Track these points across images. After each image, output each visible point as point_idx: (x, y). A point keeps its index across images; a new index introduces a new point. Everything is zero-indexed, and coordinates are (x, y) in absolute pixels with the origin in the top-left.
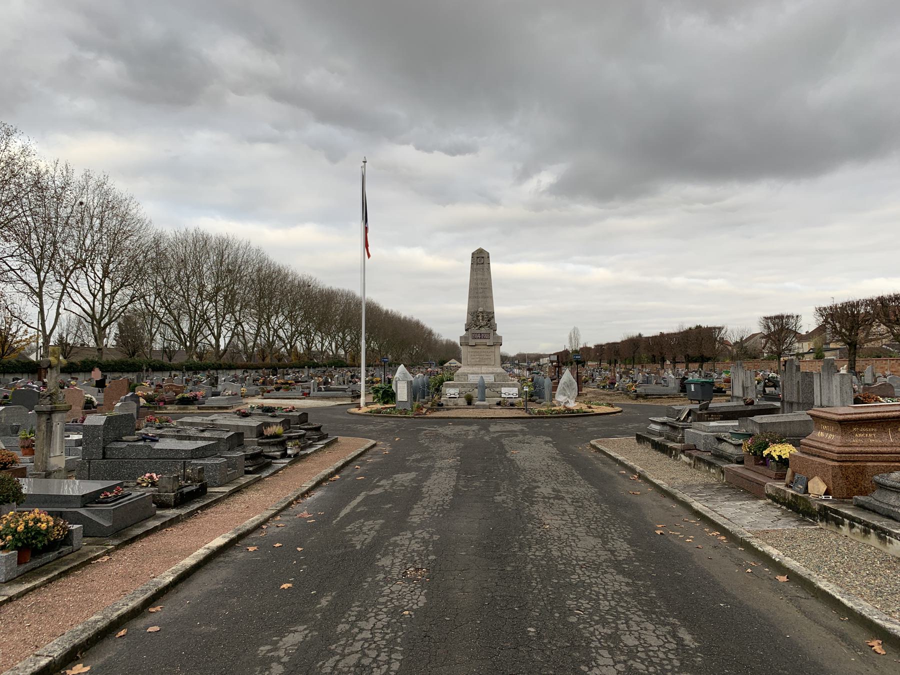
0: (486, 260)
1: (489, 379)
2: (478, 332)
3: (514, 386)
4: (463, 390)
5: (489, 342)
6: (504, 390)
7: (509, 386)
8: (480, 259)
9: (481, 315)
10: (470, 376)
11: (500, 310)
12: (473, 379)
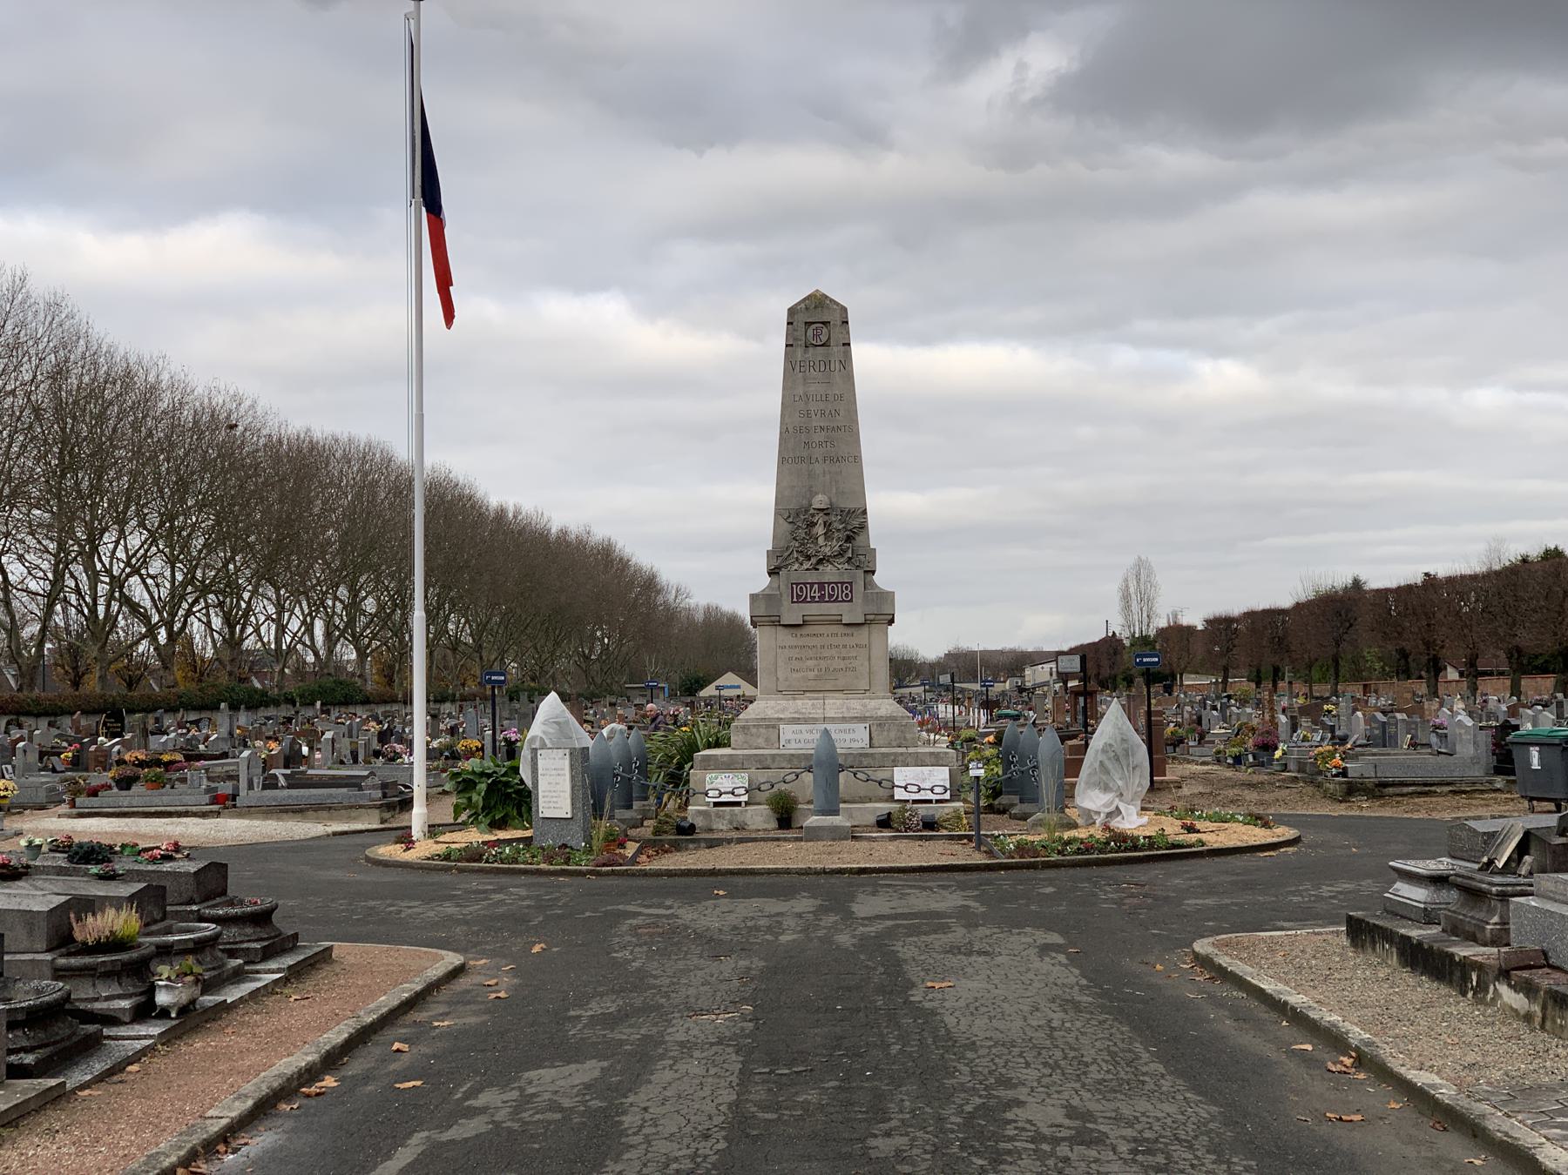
0: (836, 335)
1: (852, 739)
2: (812, 577)
3: (936, 760)
4: (762, 776)
5: (851, 613)
6: (902, 775)
7: (919, 761)
8: (817, 332)
9: (820, 519)
10: (787, 732)
11: (887, 504)
12: (798, 739)
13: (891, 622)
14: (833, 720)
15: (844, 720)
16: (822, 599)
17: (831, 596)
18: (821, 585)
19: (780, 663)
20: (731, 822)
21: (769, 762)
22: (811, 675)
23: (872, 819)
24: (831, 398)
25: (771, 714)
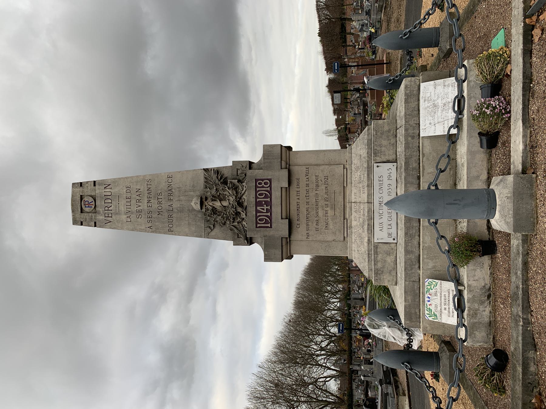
0: (88, 191)
1: (389, 179)
2: (252, 210)
3: (414, 97)
5: (280, 180)
7: (414, 113)
10: (380, 236)
12: (389, 228)
13: (289, 148)
14: (370, 195)
15: (370, 186)
16: (269, 204)
17: (266, 197)
18: (258, 204)
19: (320, 237)
20: (482, 303)
21: (413, 257)
22: (330, 213)
23: (481, 156)
24: (129, 195)
25: (364, 248)
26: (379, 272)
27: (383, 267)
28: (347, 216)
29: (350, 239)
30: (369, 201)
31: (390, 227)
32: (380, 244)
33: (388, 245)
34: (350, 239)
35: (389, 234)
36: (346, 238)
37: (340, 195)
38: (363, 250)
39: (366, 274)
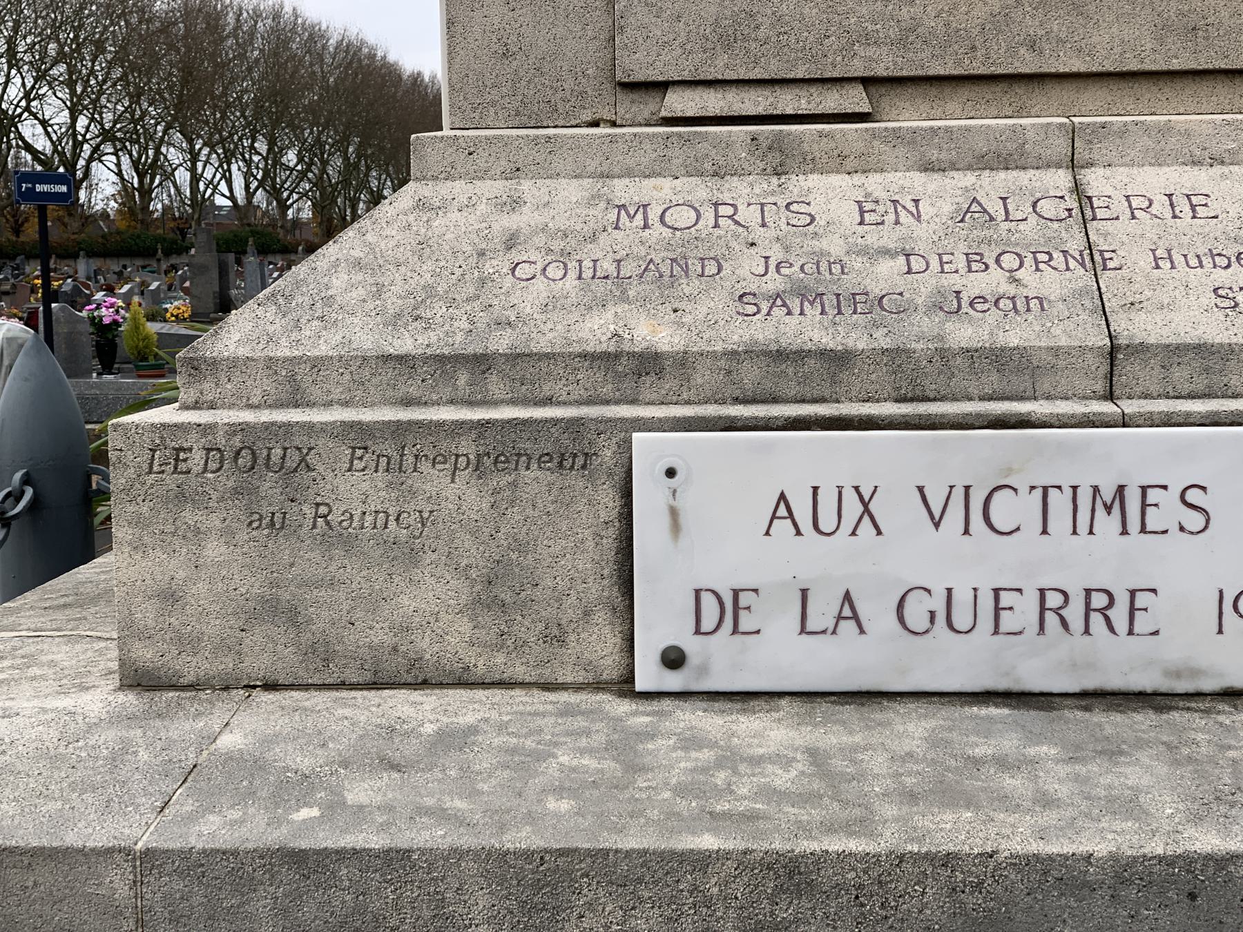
10: (715, 509)
25: (554, 312)
26: (269, 485)
27: (336, 537)
28: (908, 117)
29: (646, 156)
30: (1128, 370)
31: (821, 615)
32: (608, 500)
33: (601, 588)
34: (646, 156)
35: (732, 610)
36: (646, 106)
37: (1163, 30)
38: (530, 298)
39: (236, 336)
